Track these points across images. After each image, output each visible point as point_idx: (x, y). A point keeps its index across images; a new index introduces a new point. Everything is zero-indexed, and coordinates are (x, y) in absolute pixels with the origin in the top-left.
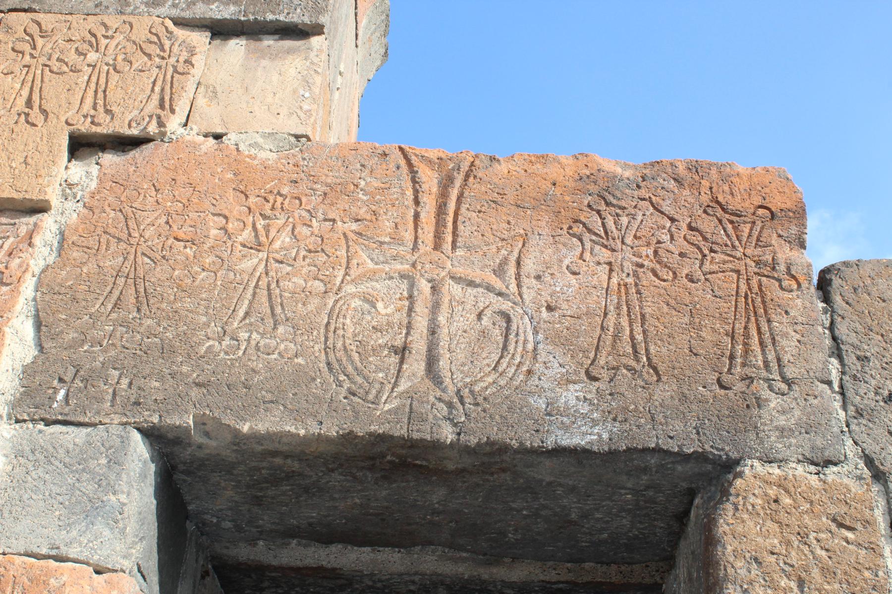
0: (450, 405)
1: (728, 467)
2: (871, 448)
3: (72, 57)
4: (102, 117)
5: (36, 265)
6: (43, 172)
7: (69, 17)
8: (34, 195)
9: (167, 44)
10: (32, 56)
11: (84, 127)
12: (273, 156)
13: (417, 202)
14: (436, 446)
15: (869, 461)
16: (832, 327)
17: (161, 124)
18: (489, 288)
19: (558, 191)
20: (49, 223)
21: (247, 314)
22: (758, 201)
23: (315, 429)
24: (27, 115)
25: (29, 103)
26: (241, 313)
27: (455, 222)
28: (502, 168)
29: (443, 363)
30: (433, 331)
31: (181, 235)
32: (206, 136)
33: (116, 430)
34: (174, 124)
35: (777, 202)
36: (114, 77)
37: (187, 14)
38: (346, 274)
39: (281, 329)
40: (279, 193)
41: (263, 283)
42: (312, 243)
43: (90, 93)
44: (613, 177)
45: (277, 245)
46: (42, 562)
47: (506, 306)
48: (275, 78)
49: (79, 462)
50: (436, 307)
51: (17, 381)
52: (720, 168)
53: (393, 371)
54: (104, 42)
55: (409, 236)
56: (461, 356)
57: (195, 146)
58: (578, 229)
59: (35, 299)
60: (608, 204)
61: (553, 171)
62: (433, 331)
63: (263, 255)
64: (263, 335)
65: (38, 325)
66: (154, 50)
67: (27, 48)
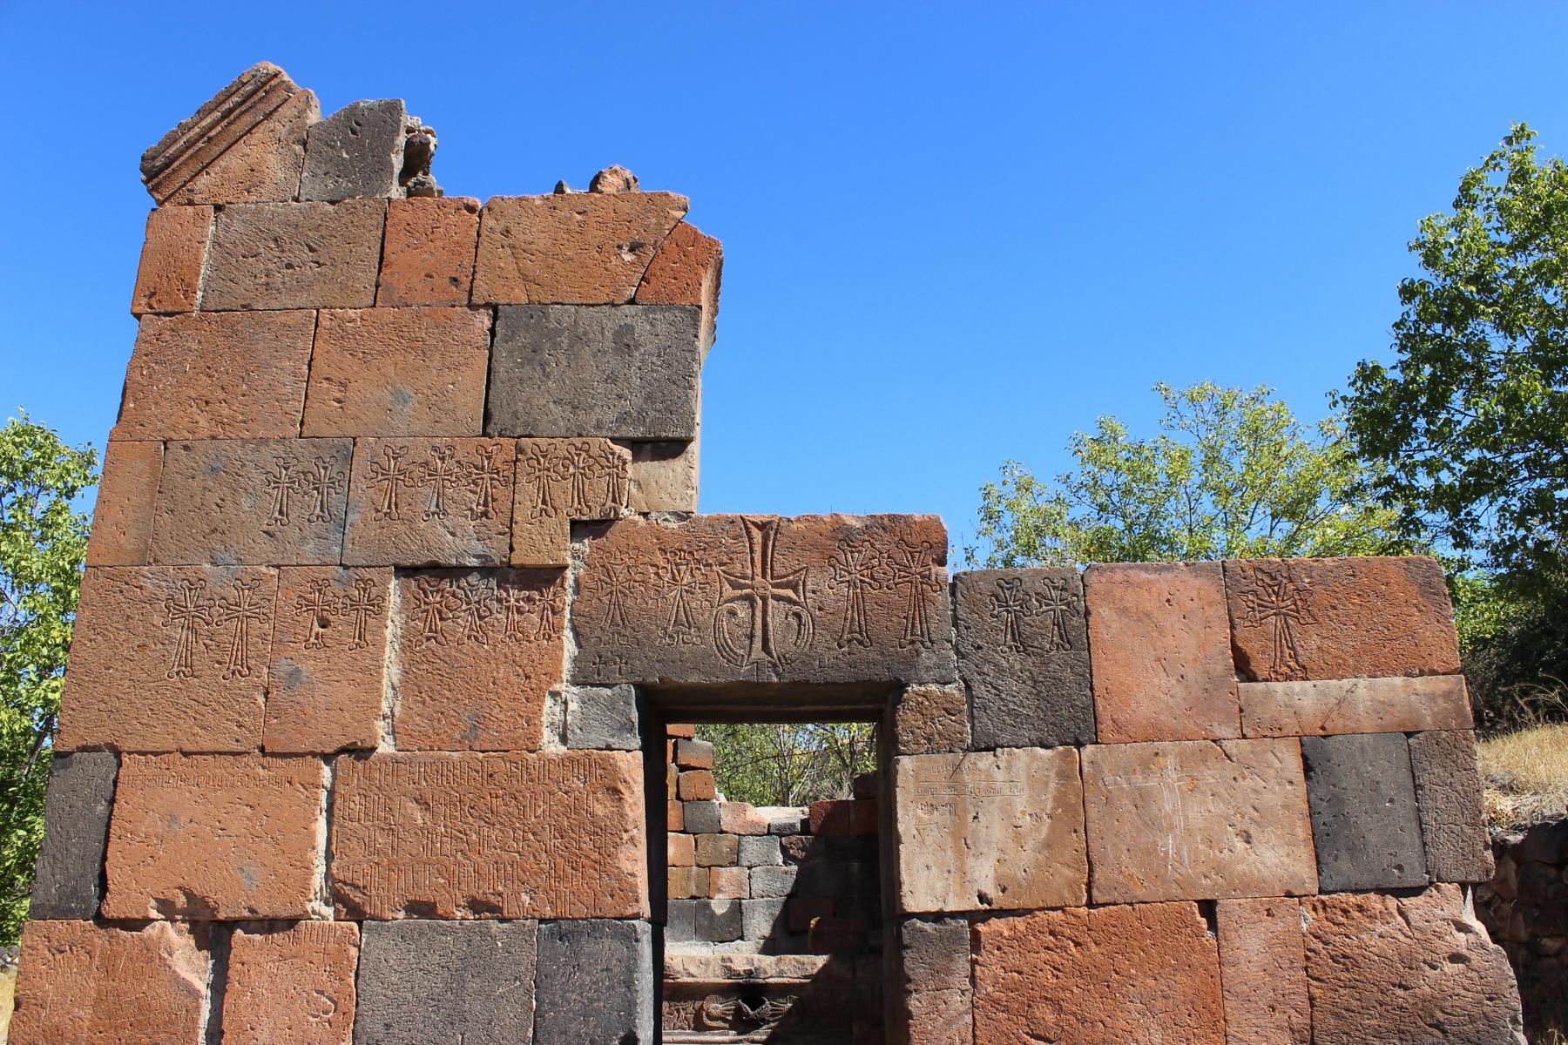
1: (900, 687)
2: (966, 673)
5: (569, 599)
8: (560, 562)
11: (577, 517)
13: (752, 551)
15: (965, 681)
16: (954, 610)
17: (616, 513)
18: (789, 600)
20: (569, 574)
22: (924, 538)
25: (544, 502)
28: (794, 526)
29: (772, 645)
30: (765, 624)
33: (624, 686)
34: (624, 511)
35: (934, 538)
36: (587, 482)
44: (850, 529)
47: (796, 608)
49: (611, 705)
52: (905, 518)
55: (749, 572)
56: (779, 637)
57: (635, 523)
58: (834, 561)
61: (821, 527)
62: (765, 624)
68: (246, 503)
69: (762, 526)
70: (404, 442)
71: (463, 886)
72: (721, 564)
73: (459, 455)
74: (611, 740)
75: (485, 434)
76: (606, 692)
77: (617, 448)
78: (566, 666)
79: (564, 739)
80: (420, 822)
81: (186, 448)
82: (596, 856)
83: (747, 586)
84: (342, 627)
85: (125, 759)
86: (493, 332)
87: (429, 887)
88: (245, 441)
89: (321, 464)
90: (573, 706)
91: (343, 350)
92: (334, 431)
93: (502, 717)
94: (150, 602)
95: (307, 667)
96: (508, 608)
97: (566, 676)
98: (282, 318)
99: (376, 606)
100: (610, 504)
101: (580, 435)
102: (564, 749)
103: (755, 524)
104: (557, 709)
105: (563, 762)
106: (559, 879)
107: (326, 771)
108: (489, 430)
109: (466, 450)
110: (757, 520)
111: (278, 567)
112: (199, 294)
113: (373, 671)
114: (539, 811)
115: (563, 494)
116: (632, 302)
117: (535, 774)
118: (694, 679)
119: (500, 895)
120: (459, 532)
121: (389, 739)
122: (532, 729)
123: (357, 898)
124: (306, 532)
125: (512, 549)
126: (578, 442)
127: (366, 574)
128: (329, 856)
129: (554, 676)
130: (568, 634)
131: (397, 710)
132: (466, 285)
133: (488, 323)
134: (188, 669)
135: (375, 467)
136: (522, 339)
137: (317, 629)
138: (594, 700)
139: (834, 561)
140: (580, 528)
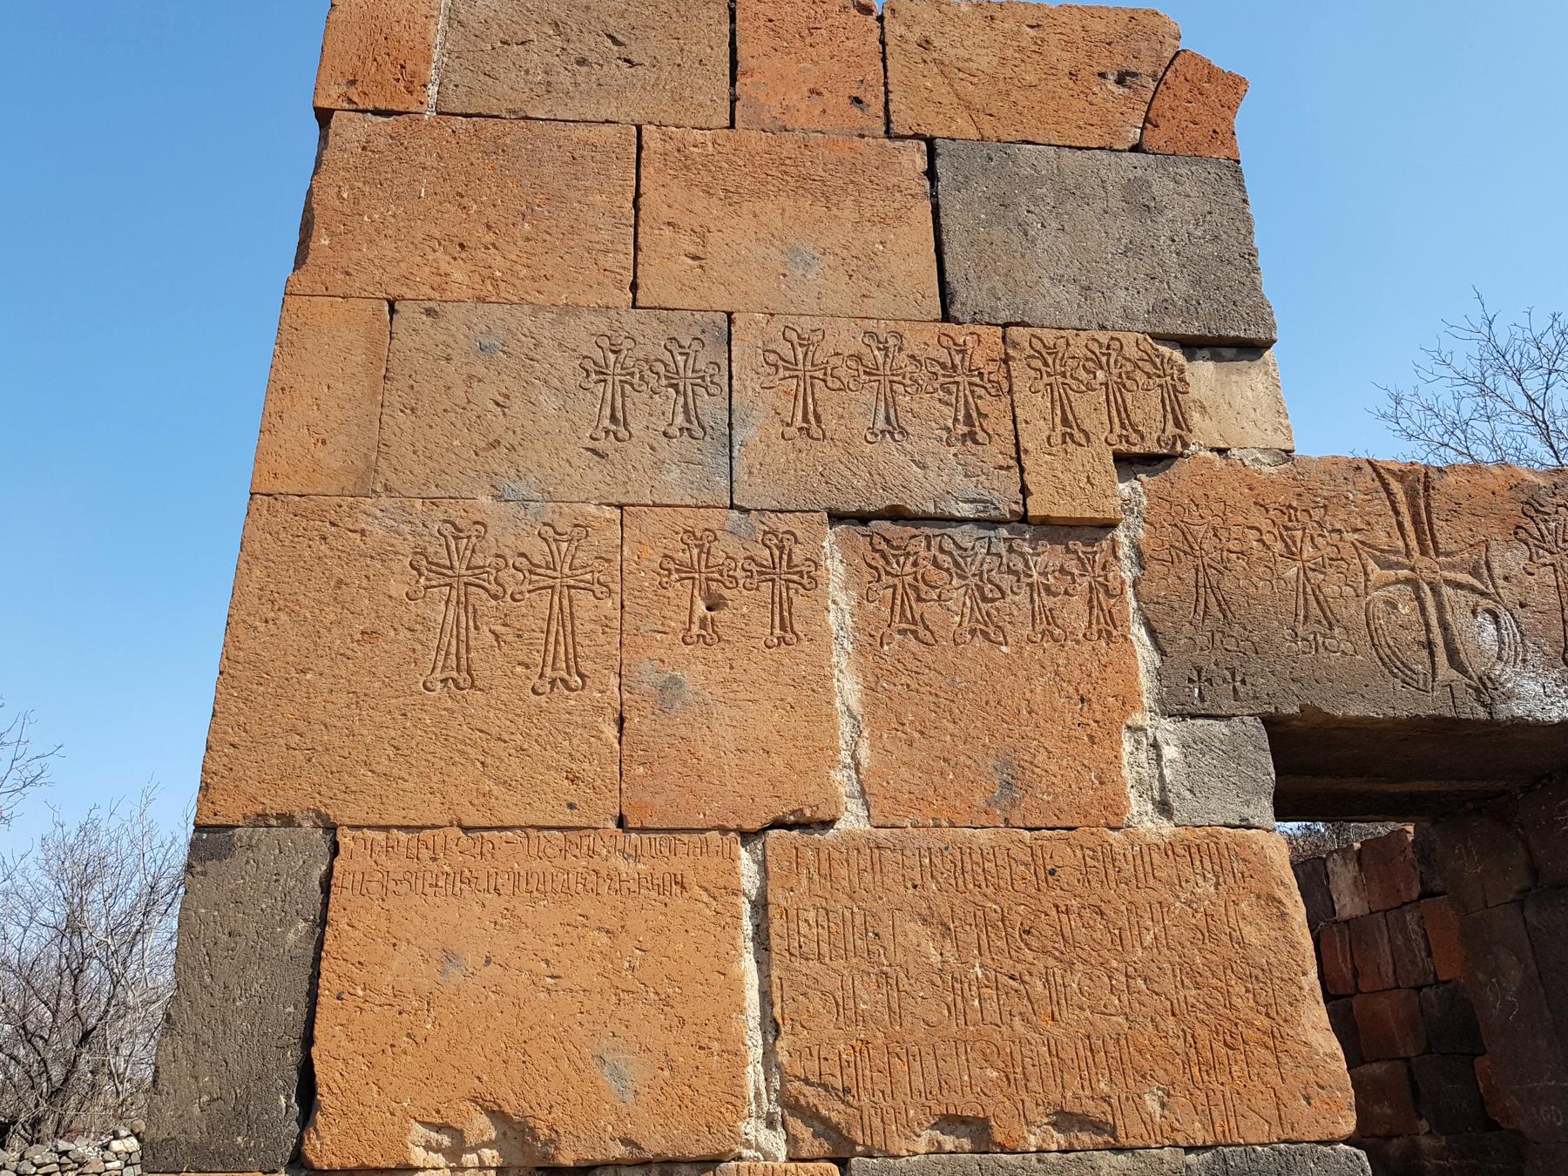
0: (1477, 690)
3: (1083, 375)
4: (1134, 437)
5: (1128, 577)
6: (1109, 492)
7: (1063, 333)
9: (1158, 361)
10: (1049, 375)
11: (1124, 447)
12: (1273, 470)
14: (1477, 722)
18: (1473, 589)
19: (1499, 499)
20: (1120, 534)
21: (1306, 617)
23: (1391, 713)
24: (1071, 435)
25: (1065, 422)
26: (1301, 618)
27: (1431, 529)
28: (1451, 479)
31: (1233, 548)
32: (1212, 450)
37: (1159, 330)
38: (1367, 580)
39: (1337, 631)
40: (1290, 506)
41: (1309, 589)
42: (1330, 551)
43: (1114, 413)
45: (1305, 556)
46: (1239, 831)
48: (1250, 393)
50: (1440, 607)
51: (1156, 683)
53: (1427, 661)
54: (1104, 359)
57: (1211, 462)
58: (1522, 534)
59: (1139, 609)
60: (1537, 511)
62: (1445, 626)
63: (1299, 564)
64: (1324, 636)
65: (1152, 633)
66: (1148, 367)
67: (1038, 364)
68: (549, 402)
69: (1401, 476)
70: (817, 323)
71: (1033, 1084)
72: (1356, 530)
73: (912, 346)
74: (1247, 812)
75: (946, 317)
76: (1219, 727)
77: (1165, 350)
78: (1145, 682)
79: (1164, 808)
80: (935, 959)
81: (429, 312)
82: (1261, 1021)
83: (1403, 566)
84: (747, 607)
85: (345, 839)
86: (931, 174)
87: (974, 1085)
88: (536, 309)
89: (674, 347)
90: (1170, 752)
91: (690, 185)
92: (690, 301)
93: (1053, 768)
94: (384, 556)
95: (693, 677)
96: (1030, 585)
97: (1147, 700)
98: (581, 132)
99: (810, 579)
100: (1171, 429)
101: (1102, 328)
102: (1167, 828)
103: (1393, 473)
104: (1143, 757)
105: (1169, 850)
106: (1210, 1067)
107: (746, 862)
108: (955, 310)
109: (925, 339)
110: (1395, 468)
111: (621, 507)
112: (433, 90)
113: (822, 682)
114: (1148, 939)
115: (1090, 410)
116: (1136, 148)
117: (1128, 870)
118: (1356, 710)
119: (1106, 1099)
120: (929, 460)
121: (855, 806)
122: (1109, 788)
123: (834, 1111)
124: (663, 454)
125: (1024, 491)
126: (1104, 337)
127: (781, 523)
128: (772, 1028)
129: (1128, 702)
130: (1139, 633)
131: (864, 753)
132: (877, 107)
133: (921, 163)
134: (463, 677)
135: (772, 358)
136: (981, 187)
137: (701, 608)
138: (1205, 744)
139: (1522, 534)
140: (1127, 463)
